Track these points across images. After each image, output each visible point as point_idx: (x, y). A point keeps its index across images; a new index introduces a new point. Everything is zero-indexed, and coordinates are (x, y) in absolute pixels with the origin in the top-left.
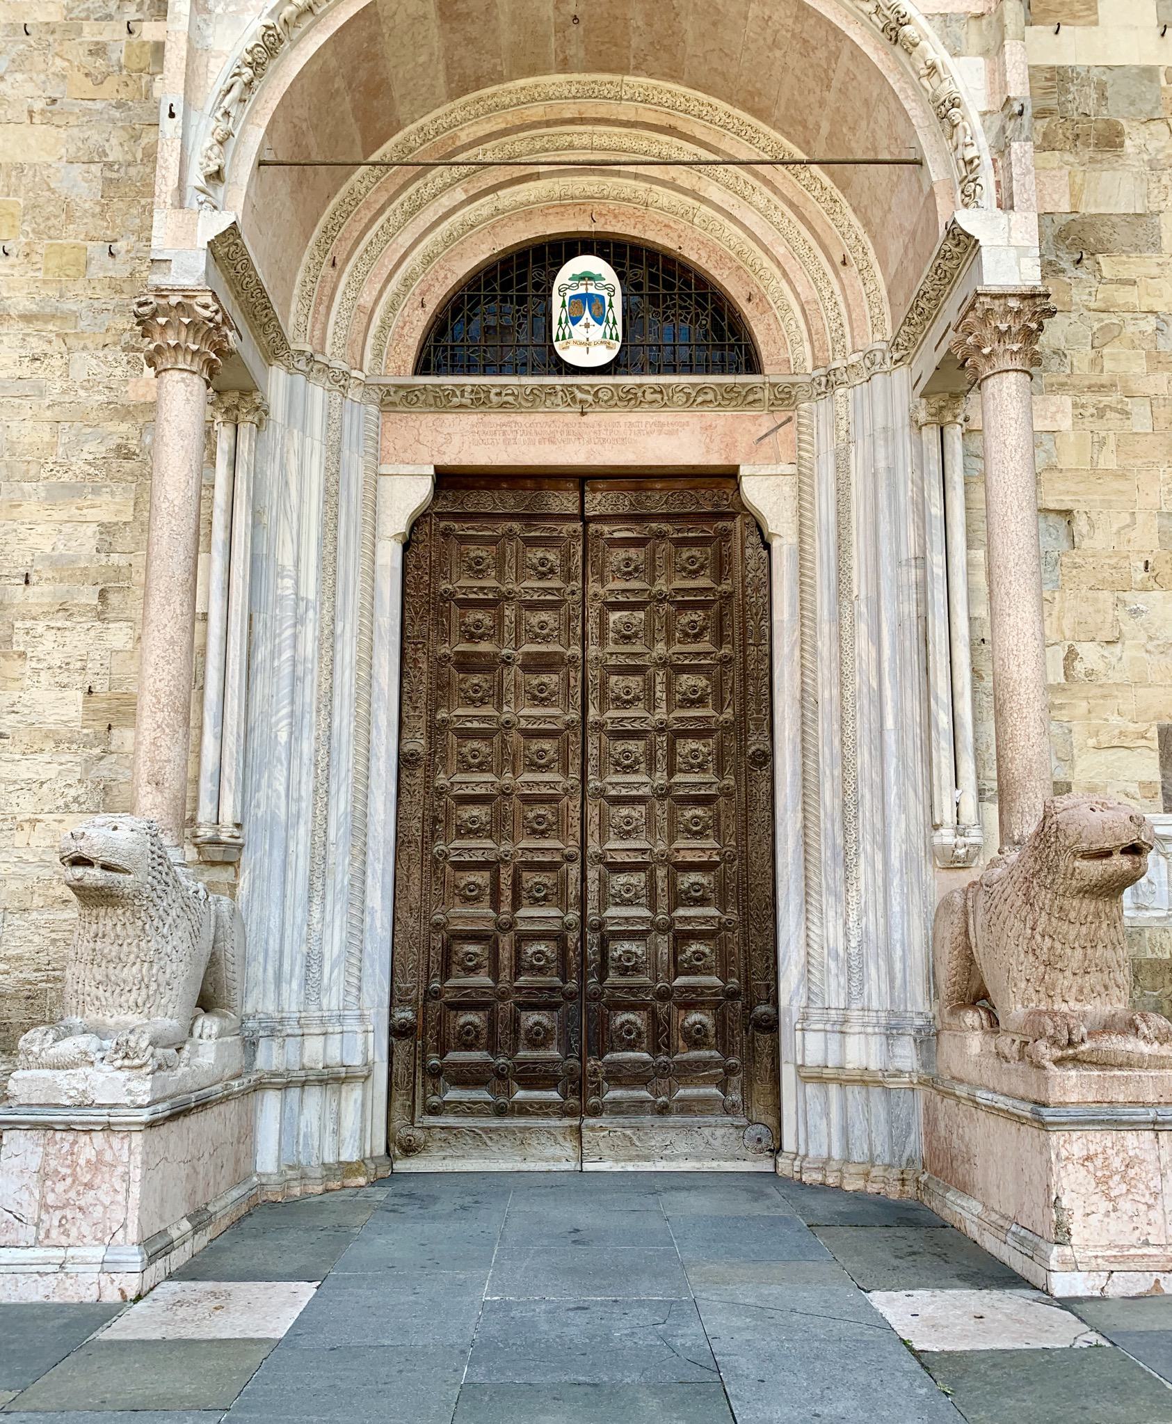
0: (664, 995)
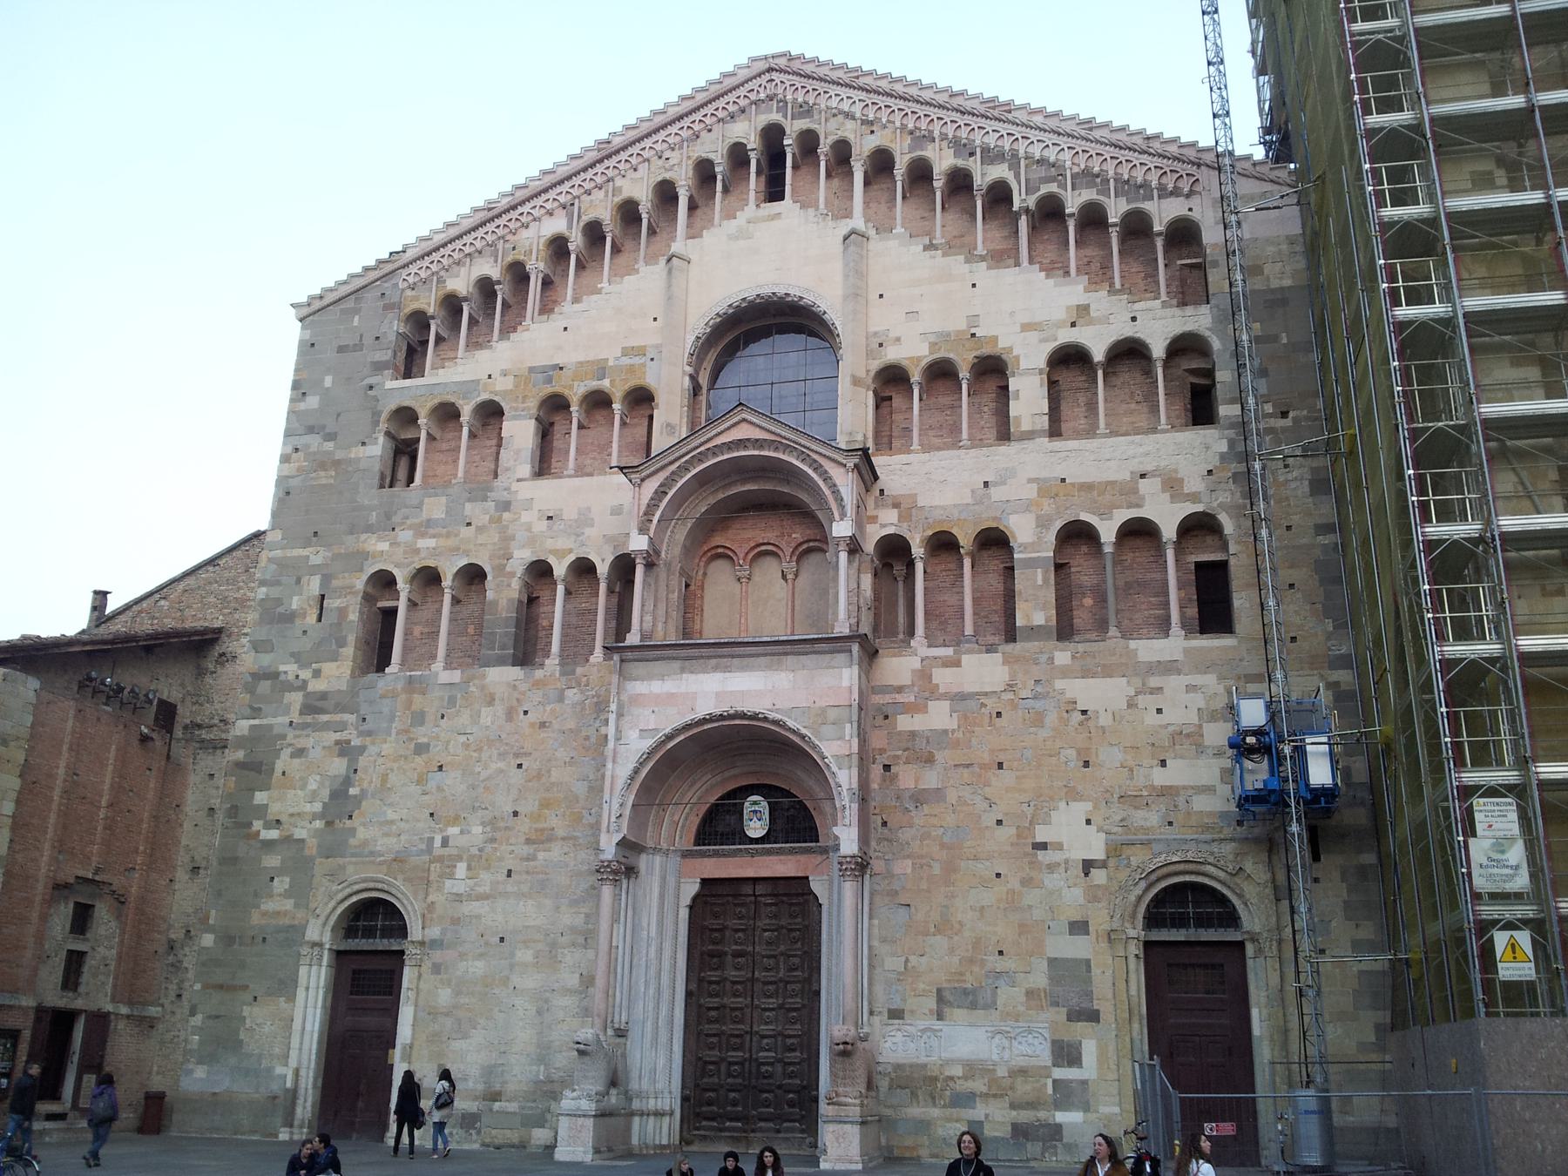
0: (780, 1087)
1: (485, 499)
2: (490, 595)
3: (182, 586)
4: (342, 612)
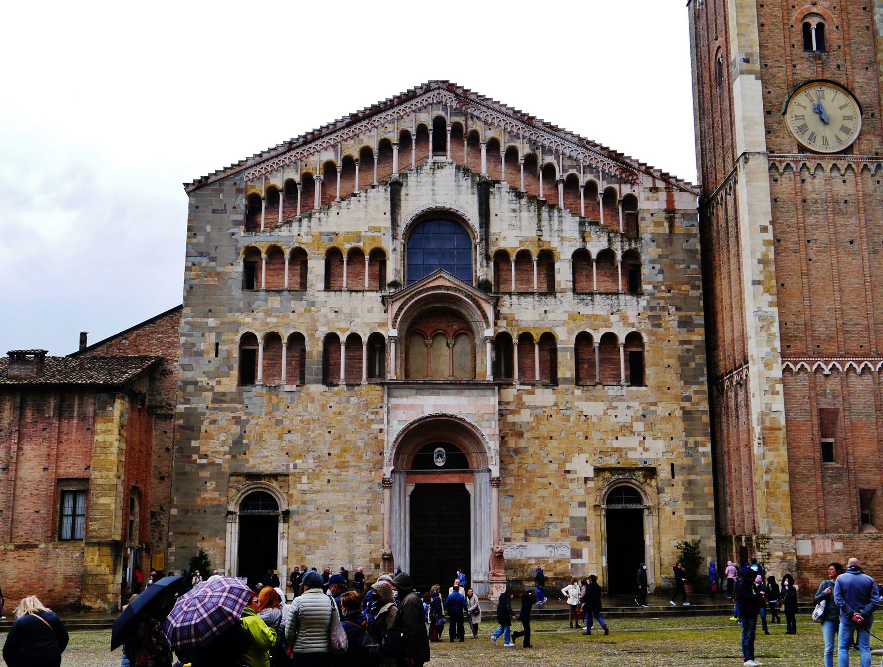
1: (302, 299)
2: (307, 349)
3: (135, 333)
4: (229, 352)
